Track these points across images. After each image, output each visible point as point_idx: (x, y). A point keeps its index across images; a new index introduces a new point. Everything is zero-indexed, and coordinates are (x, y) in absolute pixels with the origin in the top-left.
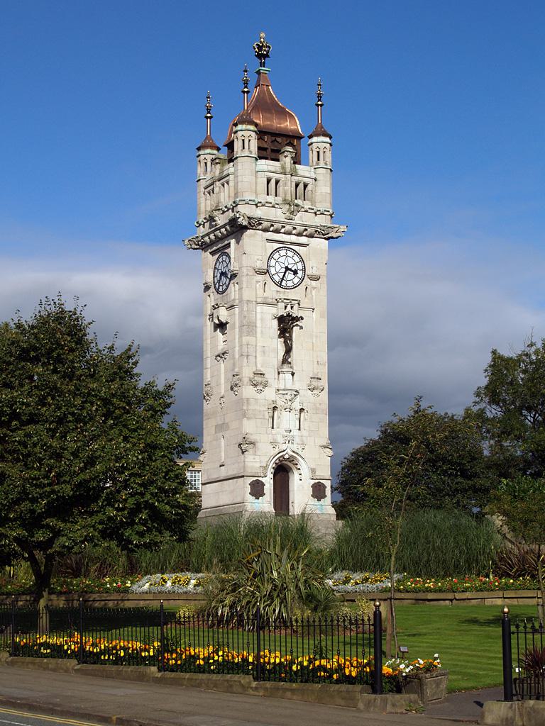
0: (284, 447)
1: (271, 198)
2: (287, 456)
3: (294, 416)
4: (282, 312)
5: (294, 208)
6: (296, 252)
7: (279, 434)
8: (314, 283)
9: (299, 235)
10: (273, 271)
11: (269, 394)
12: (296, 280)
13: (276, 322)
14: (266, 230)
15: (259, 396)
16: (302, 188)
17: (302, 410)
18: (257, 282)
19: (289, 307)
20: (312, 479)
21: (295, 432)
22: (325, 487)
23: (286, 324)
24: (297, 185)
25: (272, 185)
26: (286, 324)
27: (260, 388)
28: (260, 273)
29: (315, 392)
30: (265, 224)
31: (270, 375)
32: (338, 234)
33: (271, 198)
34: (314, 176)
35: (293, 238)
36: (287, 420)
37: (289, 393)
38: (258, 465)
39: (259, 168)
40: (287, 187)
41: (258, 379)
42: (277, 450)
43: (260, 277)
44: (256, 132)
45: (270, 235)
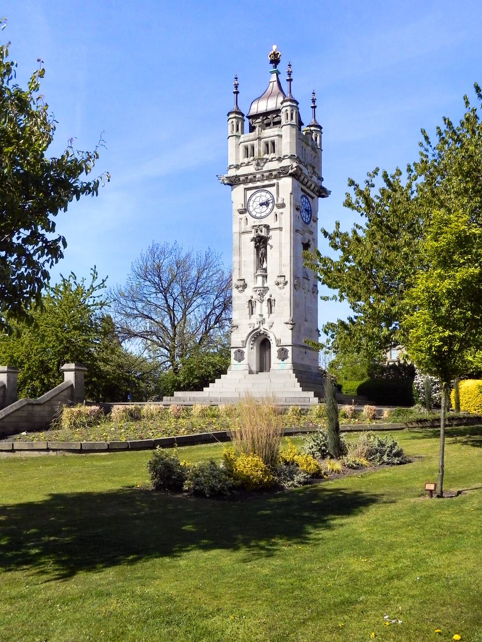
0: (256, 326)
1: (246, 160)
2: (262, 332)
3: (265, 303)
4: (253, 235)
5: (260, 162)
6: (268, 192)
7: (255, 318)
8: (281, 210)
9: (268, 178)
10: (251, 209)
11: (249, 292)
12: (268, 210)
13: (253, 243)
14: (244, 182)
15: (240, 295)
16: (271, 147)
17: (269, 300)
18: (241, 219)
19: (259, 232)
20: (277, 346)
21: (266, 316)
22: (286, 351)
23: (261, 243)
24: (267, 145)
25: (249, 151)
26: (261, 243)
27: (241, 289)
28: (242, 212)
29: (280, 286)
30: (241, 178)
31: (250, 281)
32: (293, 170)
33: (246, 160)
34: (277, 133)
35: (266, 183)
36: (261, 308)
37: (258, 289)
38: (240, 340)
39: (241, 140)
40: (259, 148)
41: (242, 283)
42: (252, 329)
43: (243, 216)
44: (235, 117)
45: (251, 185)
